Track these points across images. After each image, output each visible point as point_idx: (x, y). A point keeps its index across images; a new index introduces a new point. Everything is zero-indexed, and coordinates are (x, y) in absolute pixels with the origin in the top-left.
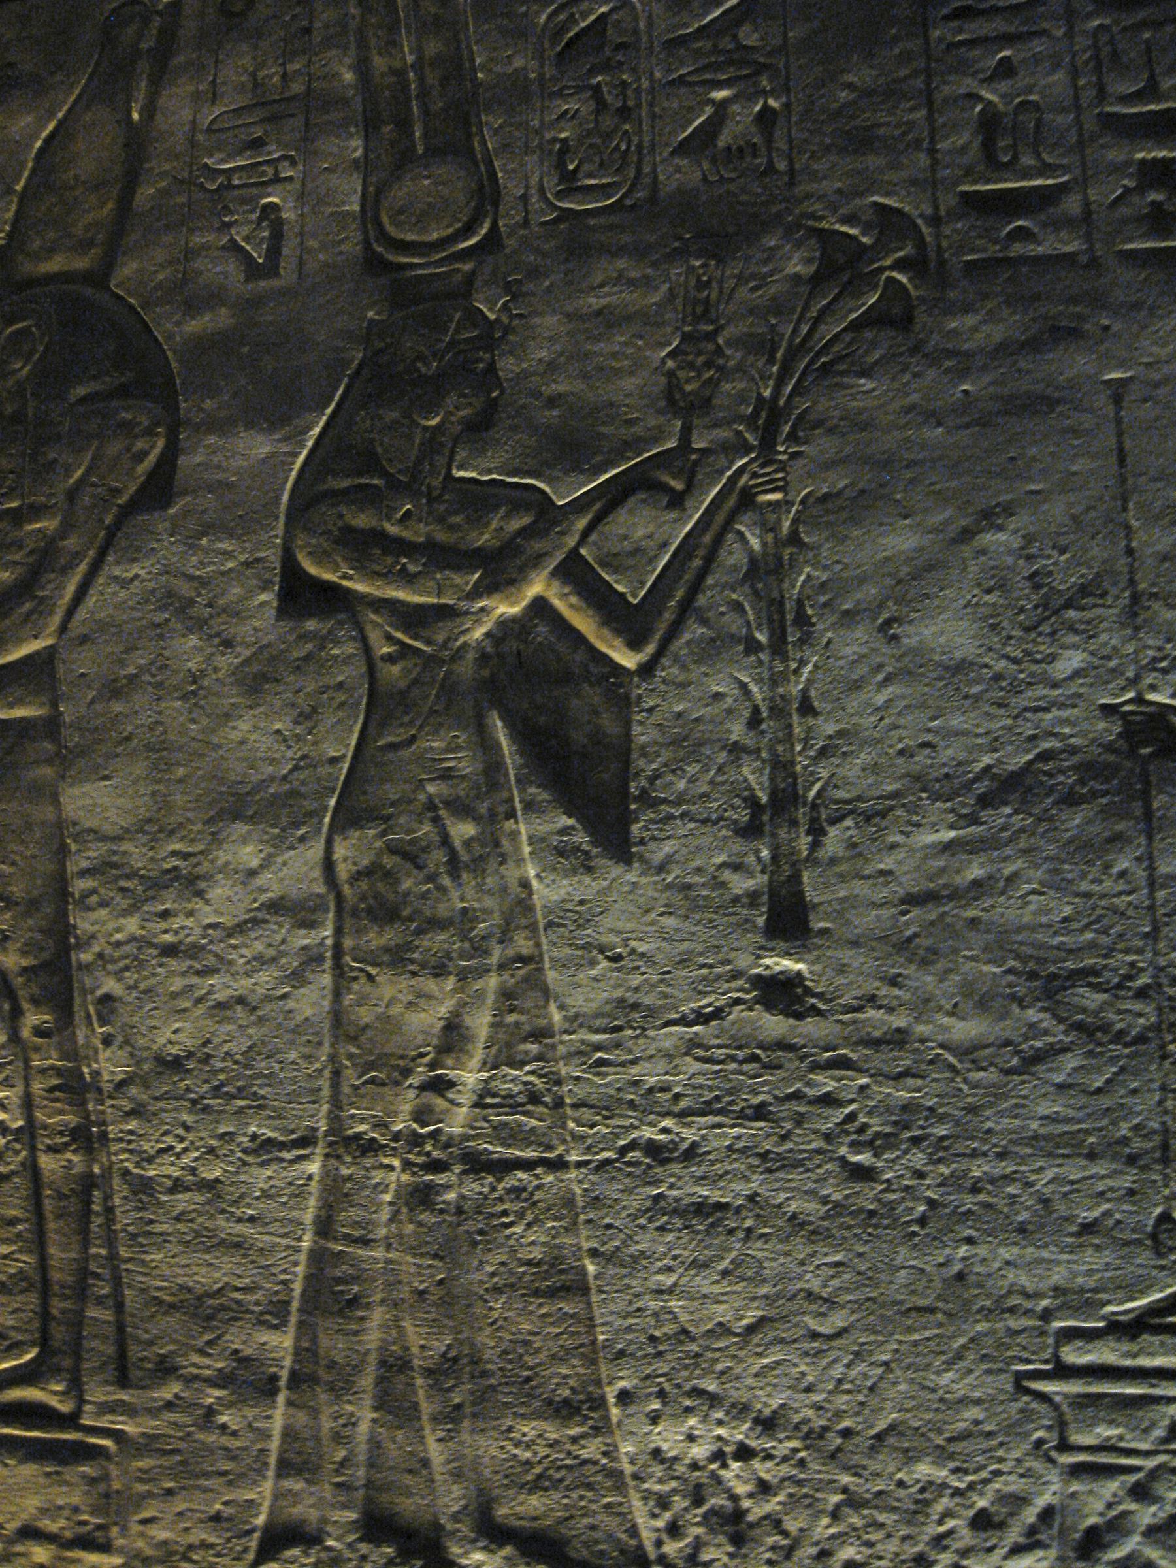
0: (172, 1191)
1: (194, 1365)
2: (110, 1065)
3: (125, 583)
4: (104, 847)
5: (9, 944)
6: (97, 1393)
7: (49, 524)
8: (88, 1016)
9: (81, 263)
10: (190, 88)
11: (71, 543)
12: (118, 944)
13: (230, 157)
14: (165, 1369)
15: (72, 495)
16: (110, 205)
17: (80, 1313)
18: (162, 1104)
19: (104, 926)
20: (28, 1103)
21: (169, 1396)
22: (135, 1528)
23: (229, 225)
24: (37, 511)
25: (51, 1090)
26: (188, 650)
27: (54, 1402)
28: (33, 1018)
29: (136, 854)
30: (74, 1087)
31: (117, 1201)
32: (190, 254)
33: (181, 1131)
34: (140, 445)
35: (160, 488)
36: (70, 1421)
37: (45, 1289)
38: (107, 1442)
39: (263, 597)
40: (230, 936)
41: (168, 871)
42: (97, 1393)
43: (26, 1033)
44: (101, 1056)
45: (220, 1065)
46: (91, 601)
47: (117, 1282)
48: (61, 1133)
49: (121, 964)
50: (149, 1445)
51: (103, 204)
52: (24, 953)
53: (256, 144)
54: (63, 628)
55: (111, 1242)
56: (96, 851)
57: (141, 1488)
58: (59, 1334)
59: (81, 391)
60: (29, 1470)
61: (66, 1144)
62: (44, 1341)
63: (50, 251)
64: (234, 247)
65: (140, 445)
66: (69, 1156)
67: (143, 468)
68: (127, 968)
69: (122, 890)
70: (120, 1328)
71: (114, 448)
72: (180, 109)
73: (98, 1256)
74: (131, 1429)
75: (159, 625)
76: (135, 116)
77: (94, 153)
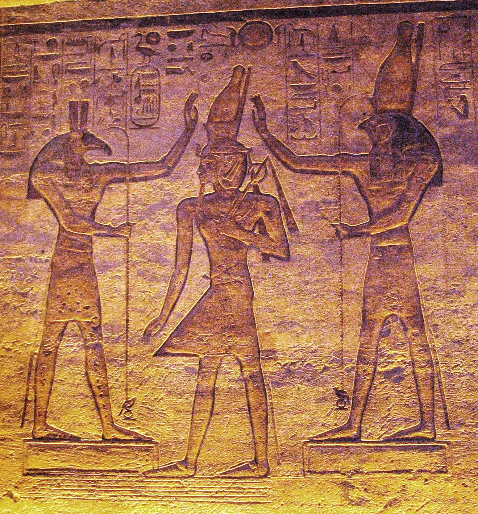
0: (459, 376)
1: (470, 422)
2: (438, 343)
3: (430, 208)
4: (431, 283)
5: (403, 311)
6: (441, 431)
7: (403, 188)
8: (430, 330)
9: (401, 107)
10: (432, 55)
11: (411, 194)
12: (438, 310)
13: (449, 79)
14: (461, 424)
15: (409, 179)
16: (409, 89)
17: (434, 411)
18: (456, 353)
19: (432, 306)
20: (411, 355)
21: (463, 431)
22: (454, 466)
23: (451, 100)
24: (396, 184)
25: (419, 351)
26: (452, 228)
27: (427, 436)
28: (411, 331)
29: (441, 284)
30: (426, 349)
31: (443, 380)
32: (439, 109)
33: (462, 360)
34: (430, 166)
35: (438, 180)
36: (433, 440)
37: (421, 405)
38: (445, 445)
39: (475, 214)
40: (472, 307)
41: (451, 290)
42: (441, 431)
43: (409, 335)
44: (435, 341)
45: (471, 342)
46: (419, 212)
47: (444, 401)
48: (424, 363)
49: (440, 315)
50: (458, 444)
51: (406, 89)
52: (407, 313)
53: (457, 76)
54: (410, 219)
55: (441, 391)
56: (428, 284)
57: (455, 456)
58: (427, 418)
59: (408, 148)
60: (422, 454)
61: (426, 365)
62: (422, 420)
63: (390, 101)
64: (454, 108)
65: (430, 166)
66: (427, 369)
67: (432, 173)
68: (441, 316)
69: (438, 295)
70: (446, 414)
71: (421, 167)
72: (428, 60)
73: (437, 395)
74: (452, 441)
75: (443, 220)
76: (413, 61)
77: (400, 72)
